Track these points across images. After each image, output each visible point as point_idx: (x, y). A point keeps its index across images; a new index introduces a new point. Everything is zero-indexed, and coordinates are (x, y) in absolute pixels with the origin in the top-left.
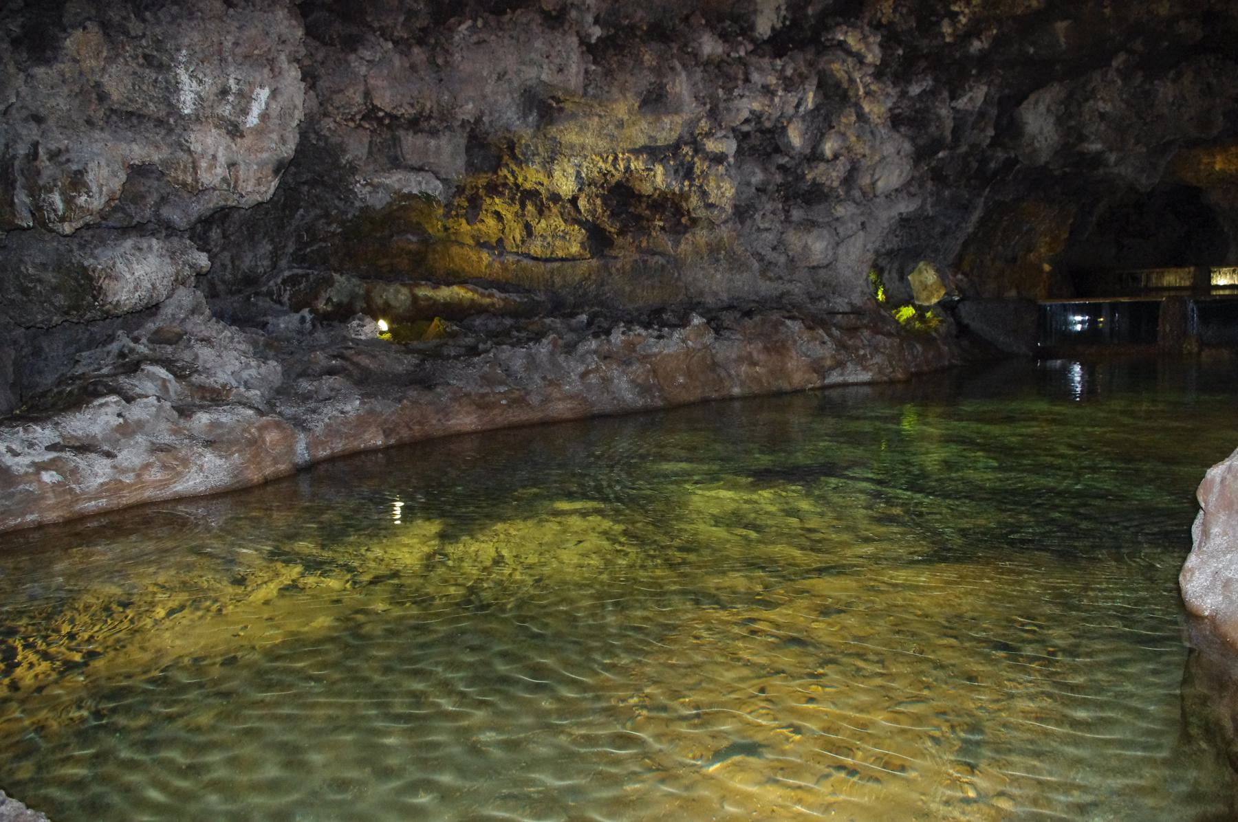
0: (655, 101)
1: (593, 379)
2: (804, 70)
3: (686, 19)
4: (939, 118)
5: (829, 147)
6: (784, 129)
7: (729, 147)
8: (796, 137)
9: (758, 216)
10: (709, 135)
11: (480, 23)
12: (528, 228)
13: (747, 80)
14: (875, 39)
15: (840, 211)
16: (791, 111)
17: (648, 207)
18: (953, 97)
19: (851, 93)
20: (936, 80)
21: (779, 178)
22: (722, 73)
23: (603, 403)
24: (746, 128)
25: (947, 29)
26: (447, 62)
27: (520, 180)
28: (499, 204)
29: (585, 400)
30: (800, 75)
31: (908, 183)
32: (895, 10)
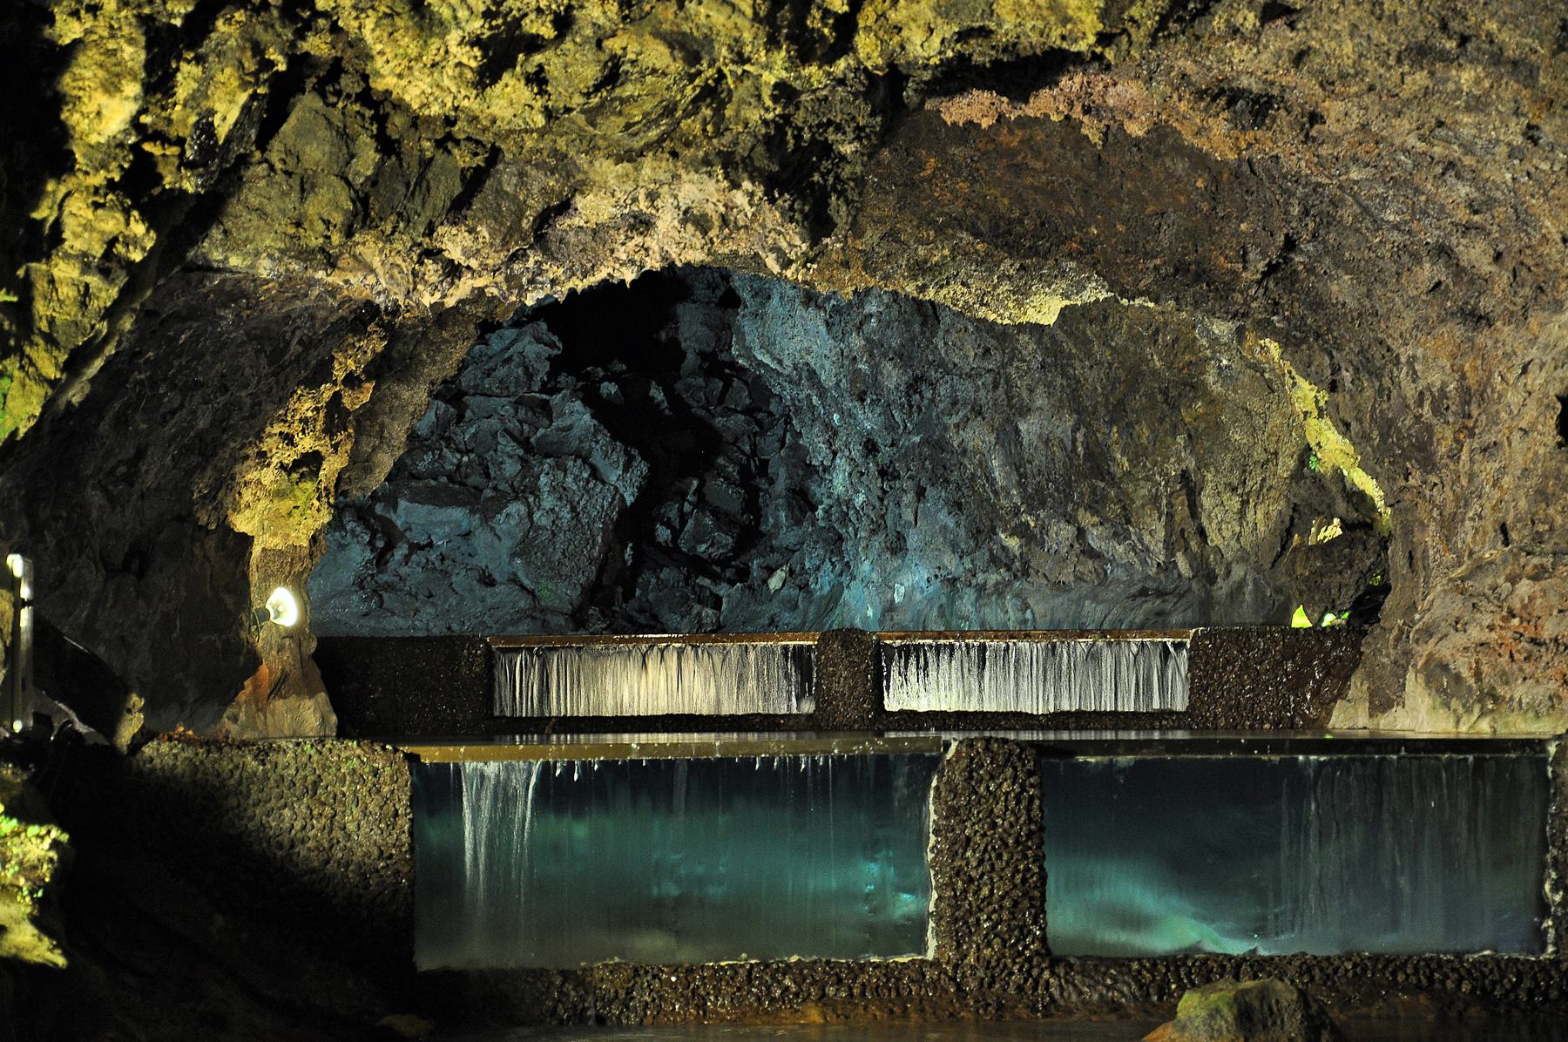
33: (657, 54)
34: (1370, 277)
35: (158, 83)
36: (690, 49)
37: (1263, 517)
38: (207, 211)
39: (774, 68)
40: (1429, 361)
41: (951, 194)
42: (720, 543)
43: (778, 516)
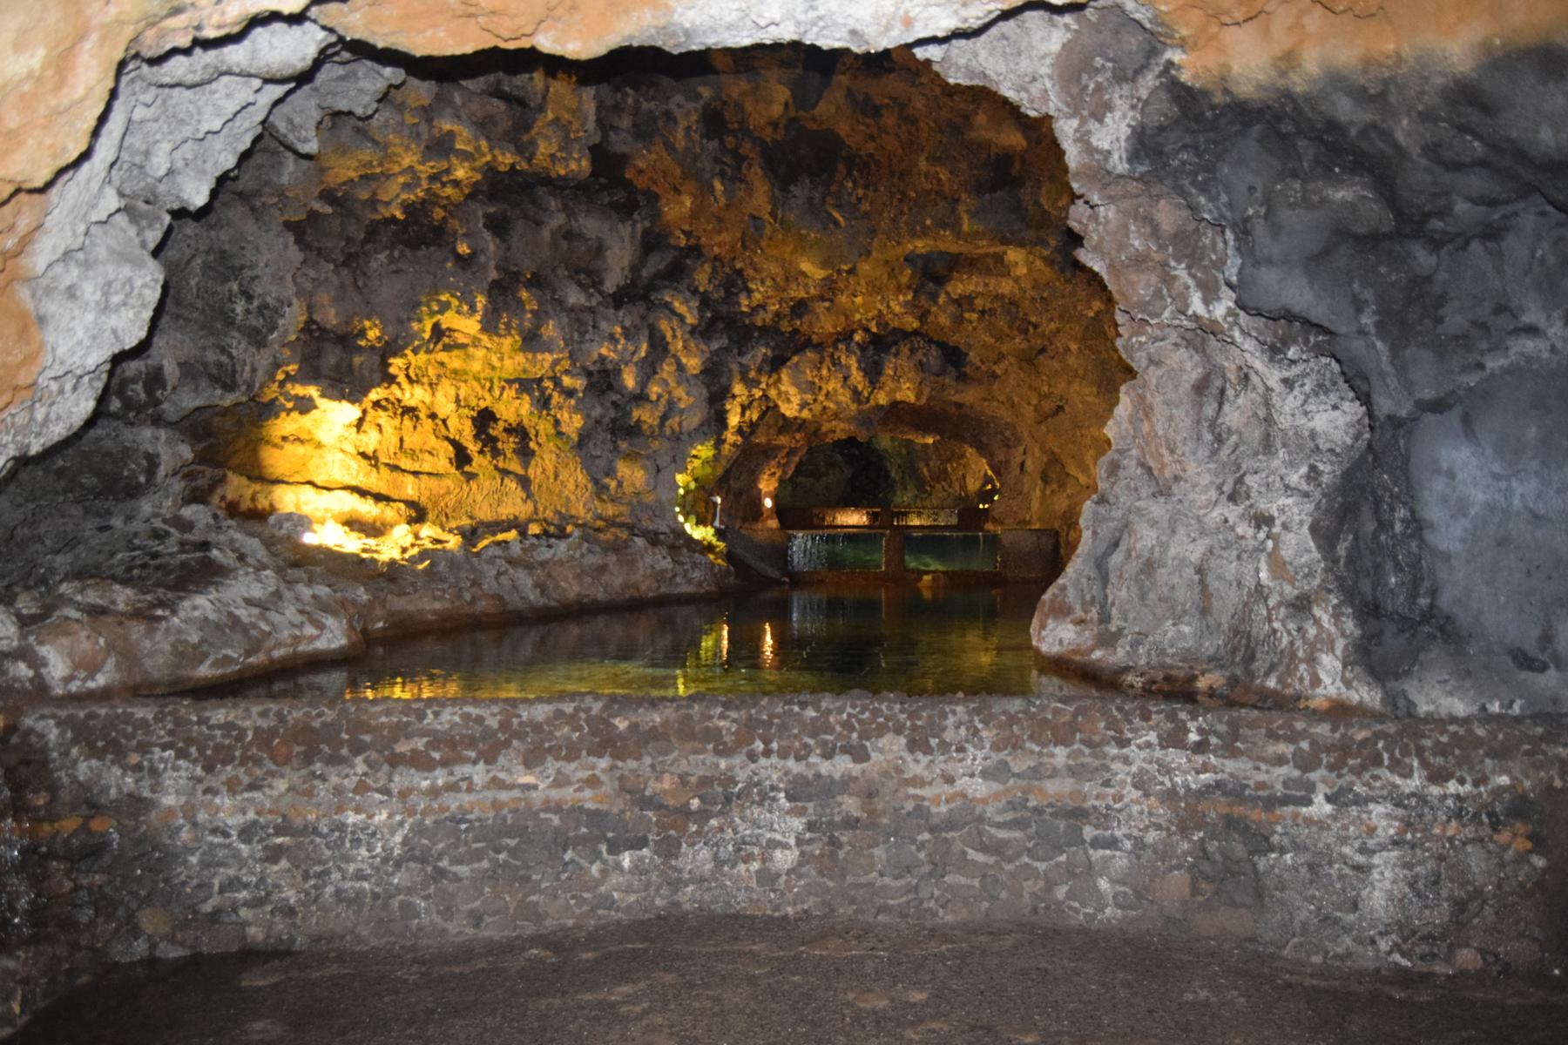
0: (531, 341)
1: (504, 580)
2: (638, 321)
3: (553, 270)
4: (730, 371)
5: (654, 390)
6: (619, 372)
7: (579, 383)
8: (629, 380)
9: (591, 445)
10: (567, 372)
12: (401, 440)
14: (695, 303)
15: (655, 445)
16: (628, 357)
17: (505, 430)
18: (741, 354)
19: (671, 347)
20: (730, 338)
21: (612, 413)
22: (581, 324)
23: (515, 602)
24: (592, 368)
25: (744, 302)
26: (366, 285)
27: (407, 395)
28: (383, 417)
29: (500, 598)
31: (702, 425)
32: (710, 281)
35: (743, 414)
36: (837, 403)
37: (978, 484)
38: (752, 433)
39: (854, 407)
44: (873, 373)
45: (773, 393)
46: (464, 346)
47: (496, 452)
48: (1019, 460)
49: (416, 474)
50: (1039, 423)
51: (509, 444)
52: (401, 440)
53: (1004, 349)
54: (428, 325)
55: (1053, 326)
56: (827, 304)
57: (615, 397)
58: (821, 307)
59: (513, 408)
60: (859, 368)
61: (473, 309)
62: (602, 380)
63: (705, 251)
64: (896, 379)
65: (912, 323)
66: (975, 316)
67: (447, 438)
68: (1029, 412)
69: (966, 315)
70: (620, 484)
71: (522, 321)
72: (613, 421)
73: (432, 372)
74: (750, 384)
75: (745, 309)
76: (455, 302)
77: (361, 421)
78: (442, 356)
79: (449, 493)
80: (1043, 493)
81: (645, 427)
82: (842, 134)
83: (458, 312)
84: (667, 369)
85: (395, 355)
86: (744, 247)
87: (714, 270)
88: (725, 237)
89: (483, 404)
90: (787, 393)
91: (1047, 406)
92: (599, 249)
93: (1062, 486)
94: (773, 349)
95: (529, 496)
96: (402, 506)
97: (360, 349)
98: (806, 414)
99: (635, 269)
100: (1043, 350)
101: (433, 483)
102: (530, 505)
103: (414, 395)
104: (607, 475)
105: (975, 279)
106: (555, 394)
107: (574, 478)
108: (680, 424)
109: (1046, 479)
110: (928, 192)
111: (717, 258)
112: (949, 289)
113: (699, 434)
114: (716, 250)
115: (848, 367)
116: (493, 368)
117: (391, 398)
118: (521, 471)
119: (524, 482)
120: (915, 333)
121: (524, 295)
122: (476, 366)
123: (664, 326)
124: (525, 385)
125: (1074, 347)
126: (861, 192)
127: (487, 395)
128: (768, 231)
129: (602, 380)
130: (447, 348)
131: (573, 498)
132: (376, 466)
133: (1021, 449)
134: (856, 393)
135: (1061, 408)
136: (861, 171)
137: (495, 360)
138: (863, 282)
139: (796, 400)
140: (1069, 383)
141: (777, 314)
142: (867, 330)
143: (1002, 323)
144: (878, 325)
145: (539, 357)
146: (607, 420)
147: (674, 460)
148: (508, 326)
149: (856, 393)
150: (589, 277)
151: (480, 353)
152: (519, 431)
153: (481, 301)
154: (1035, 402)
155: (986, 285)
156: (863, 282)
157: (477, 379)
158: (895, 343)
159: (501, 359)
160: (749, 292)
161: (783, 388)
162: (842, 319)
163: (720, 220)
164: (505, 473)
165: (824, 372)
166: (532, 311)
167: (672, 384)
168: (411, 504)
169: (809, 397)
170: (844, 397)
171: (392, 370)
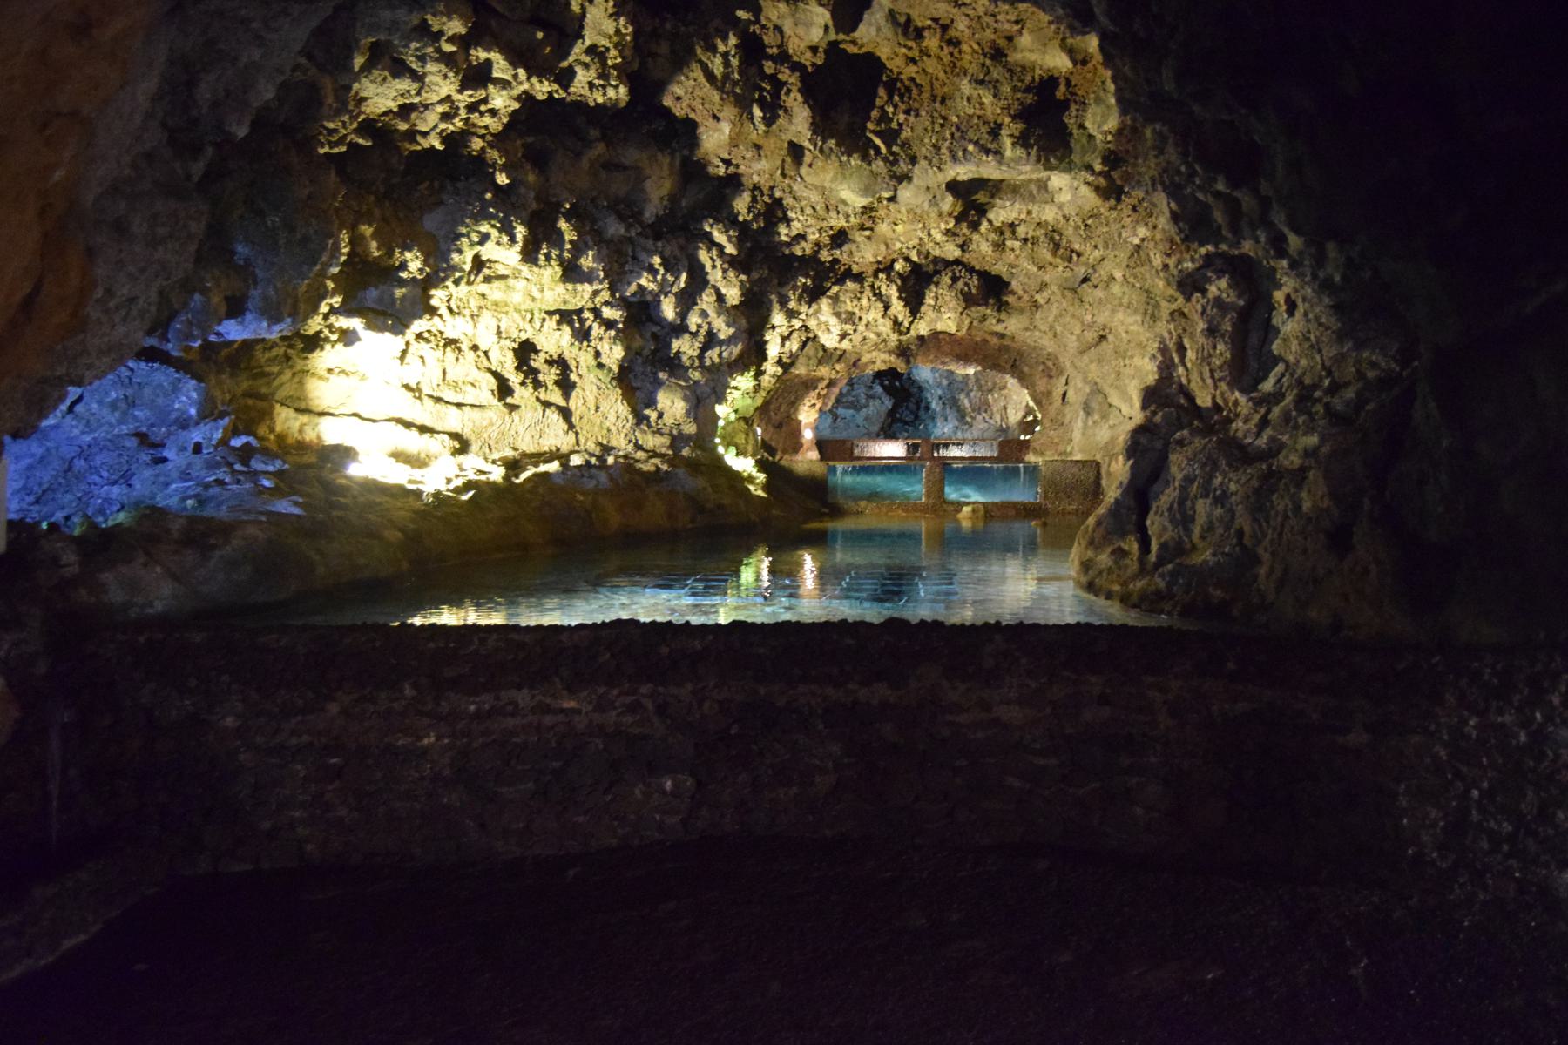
0: (571, 273)
8: (669, 310)
10: (606, 303)
11: (436, 184)
12: (444, 372)
13: (634, 258)
17: (546, 361)
19: (710, 277)
20: (770, 270)
25: (783, 230)
30: (675, 258)
33: (872, 336)
34: (1031, 367)
35: (783, 345)
36: (878, 334)
38: (792, 364)
39: (894, 337)
40: (1041, 385)
41: (946, 348)
42: (910, 418)
43: (922, 413)
44: (914, 302)
45: (812, 324)
46: (504, 277)
47: (537, 385)
48: (1061, 391)
49: (459, 405)
50: (1082, 352)
51: (550, 375)
52: (444, 372)
53: (1047, 278)
54: (468, 255)
55: (1097, 254)
56: (867, 233)
57: (656, 329)
58: (859, 237)
59: (554, 340)
60: (900, 298)
61: (513, 240)
62: (640, 313)
63: (744, 180)
64: (937, 308)
65: (952, 252)
66: (1017, 244)
67: (489, 370)
68: (1072, 343)
69: (1009, 243)
70: (660, 415)
71: (562, 250)
72: (654, 352)
73: (474, 304)
74: (791, 314)
75: (784, 238)
76: (494, 233)
77: (404, 352)
78: (484, 288)
79: (492, 424)
80: (1085, 423)
81: (684, 358)
82: (883, 58)
83: (498, 243)
84: (707, 300)
85: (436, 287)
86: (784, 175)
87: (754, 199)
88: (763, 165)
89: (524, 337)
90: (826, 324)
91: (1090, 336)
92: (639, 177)
93: (1105, 417)
94: (813, 279)
95: (571, 426)
96: (446, 437)
97: (402, 283)
98: (846, 345)
99: (673, 198)
100: (1085, 280)
101: (476, 413)
102: (572, 435)
103: (453, 327)
104: (648, 406)
105: (1017, 205)
106: (596, 325)
107: (616, 409)
108: (720, 355)
109: (1088, 410)
110: (971, 116)
111: (756, 187)
112: (991, 215)
113: (739, 365)
114: (756, 178)
115: (889, 297)
116: (534, 299)
117: (434, 331)
118: (562, 403)
119: (566, 414)
120: (957, 262)
121: (563, 225)
122: (517, 298)
123: (703, 255)
124: (565, 316)
125: (1118, 275)
126: (902, 117)
127: (528, 326)
128: (807, 159)
129: (640, 313)
130: (488, 280)
131: (614, 429)
132: (419, 398)
133: (1063, 380)
134: (896, 323)
135: (1103, 337)
136: (901, 96)
137: (537, 295)
138: (903, 210)
139: (836, 330)
140: (1113, 311)
141: (817, 244)
142: (907, 259)
143: (1045, 253)
144: (919, 253)
145: (579, 287)
146: (646, 352)
147: (714, 390)
148: (548, 257)
149: (896, 323)
150: (628, 210)
151: (520, 285)
152: (560, 363)
153: (521, 231)
154: (1078, 331)
155: (1029, 213)
156: (903, 210)
157: (518, 310)
158: (937, 272)
159: (542, 290)
160: (788, 221)
161: (823, 319)
162: (883, 247)
163: (758, 147)
164: (547, 404)
165: (865, 302)
166: (571, 242)
167: (712, 314)
168: (455, 436)
169: (849, 328)
170: (885, 327)
171: (434, 302)
